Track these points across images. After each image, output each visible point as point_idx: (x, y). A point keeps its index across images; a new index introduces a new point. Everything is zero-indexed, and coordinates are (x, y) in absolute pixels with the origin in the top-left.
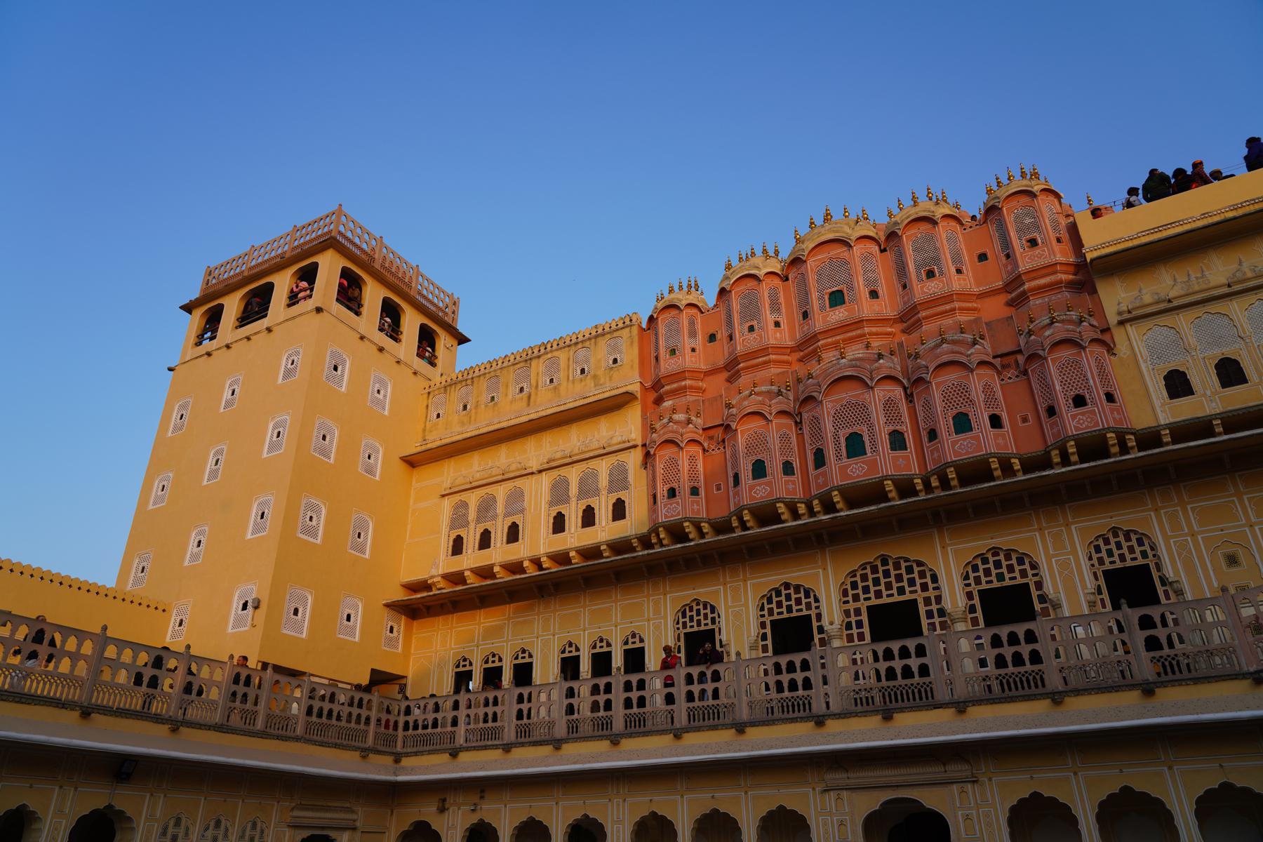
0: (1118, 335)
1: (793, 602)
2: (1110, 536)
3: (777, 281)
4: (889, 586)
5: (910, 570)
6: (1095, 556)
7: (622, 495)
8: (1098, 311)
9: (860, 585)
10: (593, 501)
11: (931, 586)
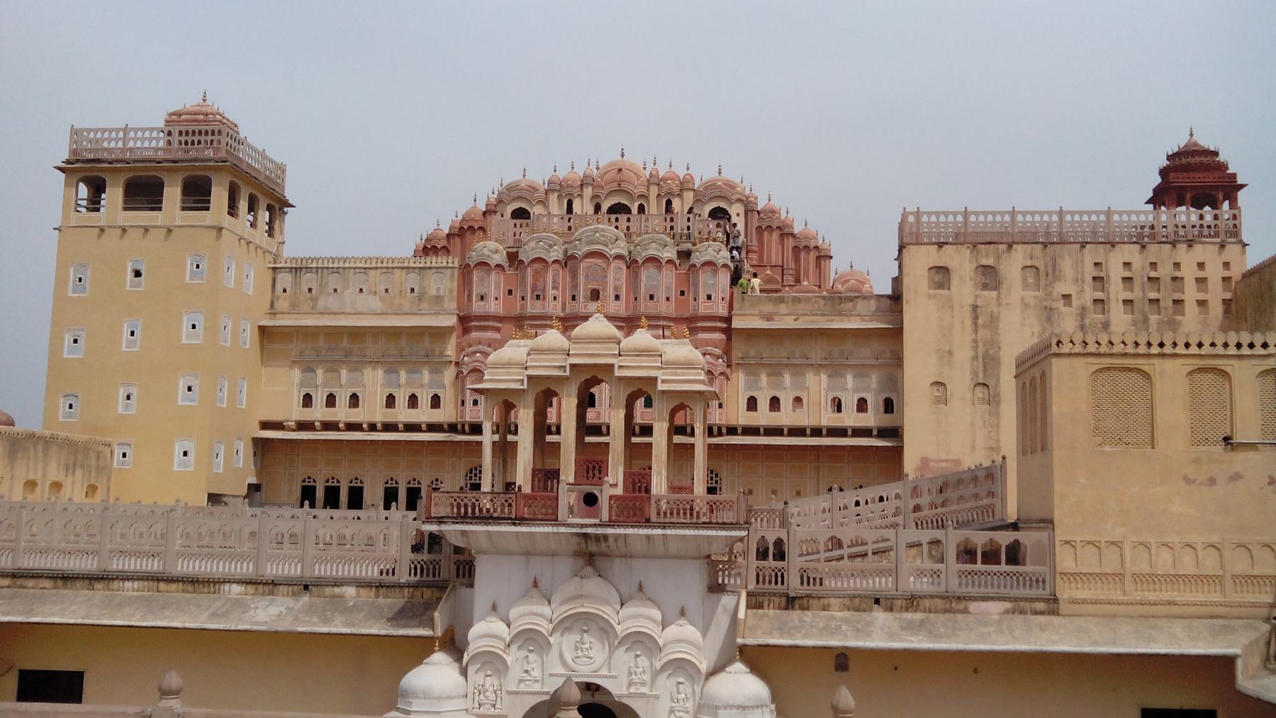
3: (557, 266)
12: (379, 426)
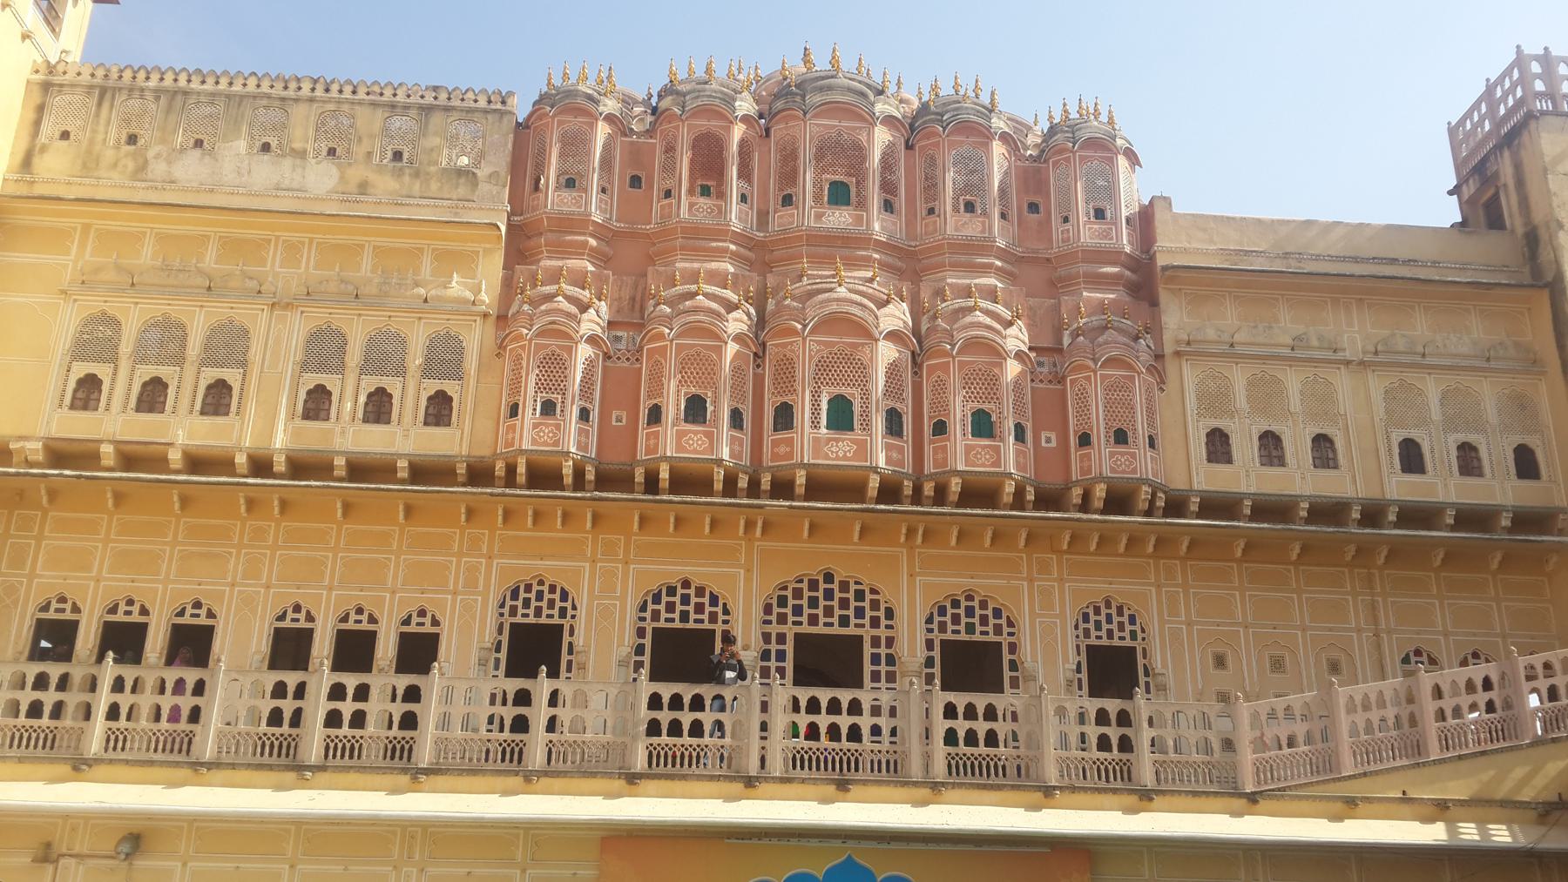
0: (1171, 367)
1: (691, 608)
2: (1103, 606)
4: (829, 612)
5: (860, 595)
6: (1082, 626)
7: (451, 387)
8: (1153, 328)
9: (791, 602)
10: (393, 385)
11: (883, 622)
12: (280, 464)
